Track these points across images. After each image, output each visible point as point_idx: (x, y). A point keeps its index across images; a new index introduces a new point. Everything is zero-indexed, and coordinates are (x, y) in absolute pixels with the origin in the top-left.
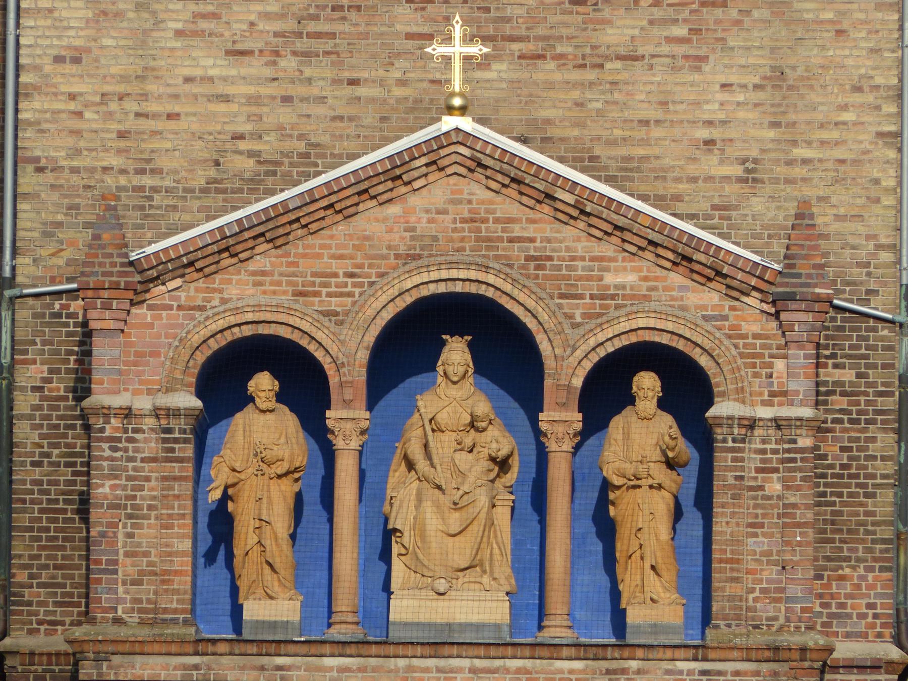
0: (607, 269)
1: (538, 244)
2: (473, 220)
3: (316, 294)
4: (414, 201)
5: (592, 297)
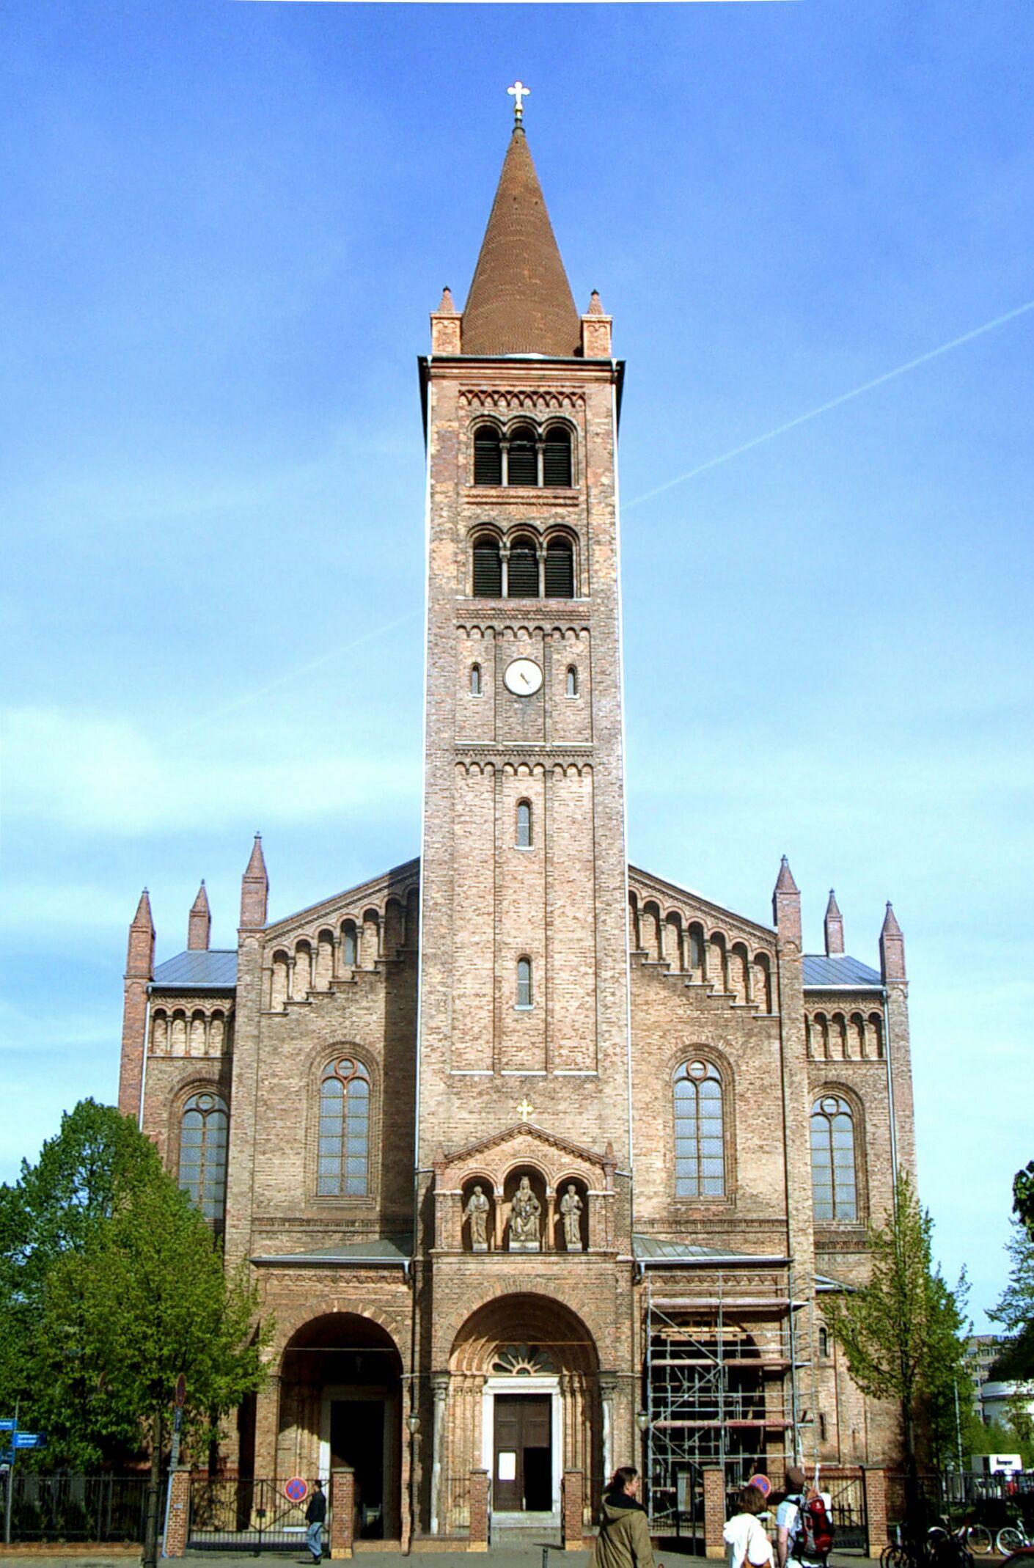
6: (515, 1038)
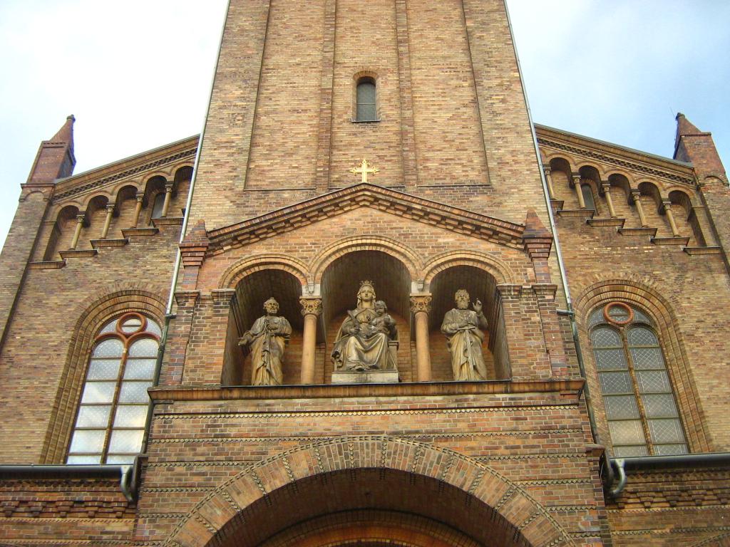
0: (440, 237)
1: (405, 229)
2: (372, 222)
3: (296, 251)
4: (344, 216)
5: (433, 247)
6: (352, 152)
